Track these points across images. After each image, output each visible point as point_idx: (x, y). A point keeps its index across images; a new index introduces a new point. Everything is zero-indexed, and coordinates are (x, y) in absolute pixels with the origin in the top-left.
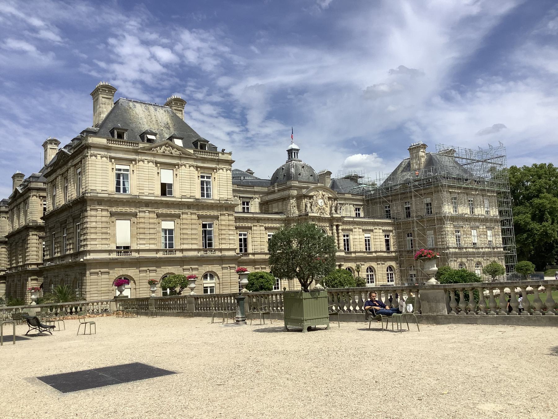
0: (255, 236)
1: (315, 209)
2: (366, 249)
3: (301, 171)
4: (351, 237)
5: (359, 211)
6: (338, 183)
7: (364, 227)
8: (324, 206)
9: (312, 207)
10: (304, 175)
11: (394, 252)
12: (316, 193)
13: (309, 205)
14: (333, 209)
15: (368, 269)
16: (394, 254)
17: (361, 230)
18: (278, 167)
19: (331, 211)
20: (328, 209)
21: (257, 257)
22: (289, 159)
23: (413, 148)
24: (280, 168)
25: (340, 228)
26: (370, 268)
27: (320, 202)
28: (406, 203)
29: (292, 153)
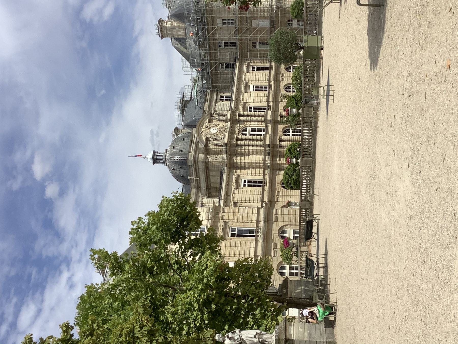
0: (244, 199)
1: (221, 136)
2: (266, 90)
3: (178, 149)
4: (252, 105)
5: (223, 97)
6: (189, 121)
7: (243, 91)
8: (218, 127)
9: (218, 138)
10: (182, 146)
11: (271, 63)
12: (203, 134)
13: (216, 142)
14: (221, 118)
15: (287, 91)
16: (273, 64)
17: (246, 94)
18: (171, 175)
19: (223, 121)
20: (222, 124)
21: (266, 199)
22: (163, 163)
23: (162, 33)
24: (172, 173)
25: (242, 113)
26: (286, 88)
27: (213, 131)
28: (220, 46)
29: (157, 159)
